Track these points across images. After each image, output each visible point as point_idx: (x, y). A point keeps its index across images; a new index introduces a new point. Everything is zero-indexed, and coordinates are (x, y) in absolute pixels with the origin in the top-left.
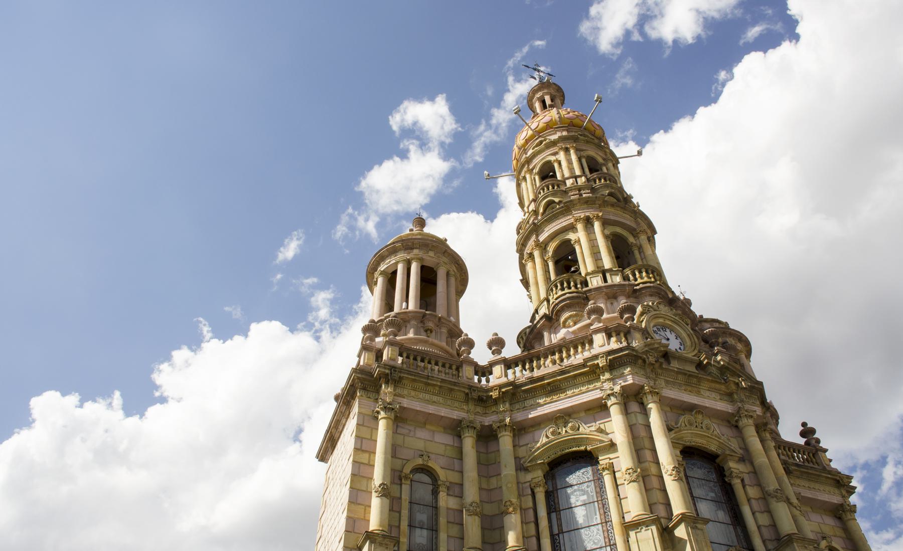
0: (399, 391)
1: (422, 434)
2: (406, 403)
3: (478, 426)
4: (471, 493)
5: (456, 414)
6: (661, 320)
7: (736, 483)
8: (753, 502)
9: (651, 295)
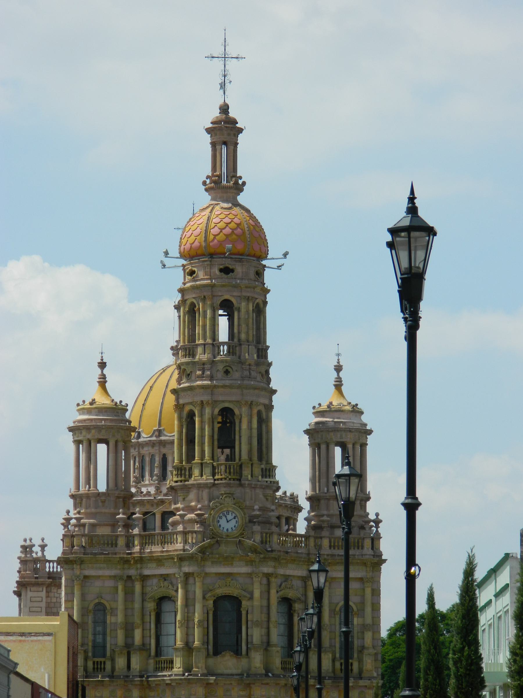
0: (83, 566)
1: (98, 583)
2: (87, 573)
3: (125, 578)
4: (120, 618)
5: (113, 572)
6: (225, 509)
7: (244, 613)
8: (249, 623)
9: (225, 487)
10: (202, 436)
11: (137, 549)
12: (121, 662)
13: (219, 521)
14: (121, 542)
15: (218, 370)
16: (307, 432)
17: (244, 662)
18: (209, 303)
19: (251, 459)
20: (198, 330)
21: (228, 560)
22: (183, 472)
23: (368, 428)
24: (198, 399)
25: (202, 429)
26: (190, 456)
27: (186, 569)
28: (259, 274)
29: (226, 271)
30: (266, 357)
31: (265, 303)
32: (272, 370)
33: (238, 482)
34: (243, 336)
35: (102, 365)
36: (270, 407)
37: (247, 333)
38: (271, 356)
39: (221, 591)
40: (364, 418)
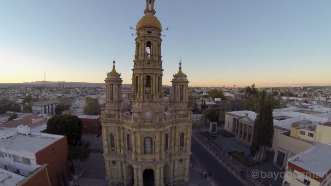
2: (107, 125)
10: (140, 85)
11: (121, 119)
12: (118, 150)
13: (145, 114)
14: (117, 116)
15: (145, 63)
16: (171, 82)
17: (153, 156)
18: (143, 42)
19: (156, 93)
20: (140, 50)
21: (148, 127)
22: (134, 96)
23: (188, 81)
24: (139, 73)
25: (140, 82)
26: (137, 92)
27: (134, 130)
28: (160, 34)
29: (149, 32)
30: (161, 59)
31: (161, 44)
32: (162, 64)
33: (151, 101)
34: (154, 52)
35: (114, 62)
36: (161, 75)
37: (155, 52)
38: (163, 59)
39: (146, 136)
40: (187, 78)
